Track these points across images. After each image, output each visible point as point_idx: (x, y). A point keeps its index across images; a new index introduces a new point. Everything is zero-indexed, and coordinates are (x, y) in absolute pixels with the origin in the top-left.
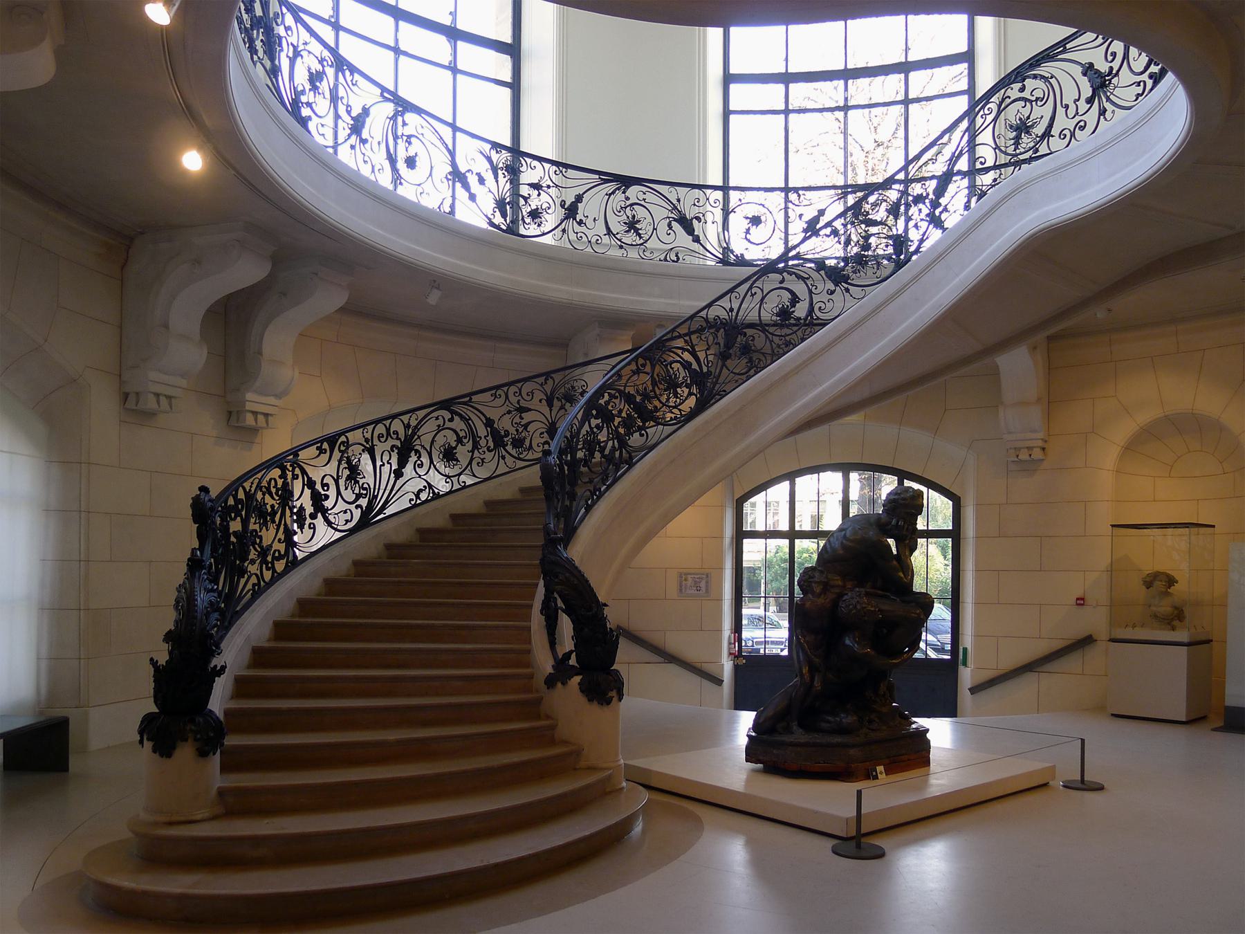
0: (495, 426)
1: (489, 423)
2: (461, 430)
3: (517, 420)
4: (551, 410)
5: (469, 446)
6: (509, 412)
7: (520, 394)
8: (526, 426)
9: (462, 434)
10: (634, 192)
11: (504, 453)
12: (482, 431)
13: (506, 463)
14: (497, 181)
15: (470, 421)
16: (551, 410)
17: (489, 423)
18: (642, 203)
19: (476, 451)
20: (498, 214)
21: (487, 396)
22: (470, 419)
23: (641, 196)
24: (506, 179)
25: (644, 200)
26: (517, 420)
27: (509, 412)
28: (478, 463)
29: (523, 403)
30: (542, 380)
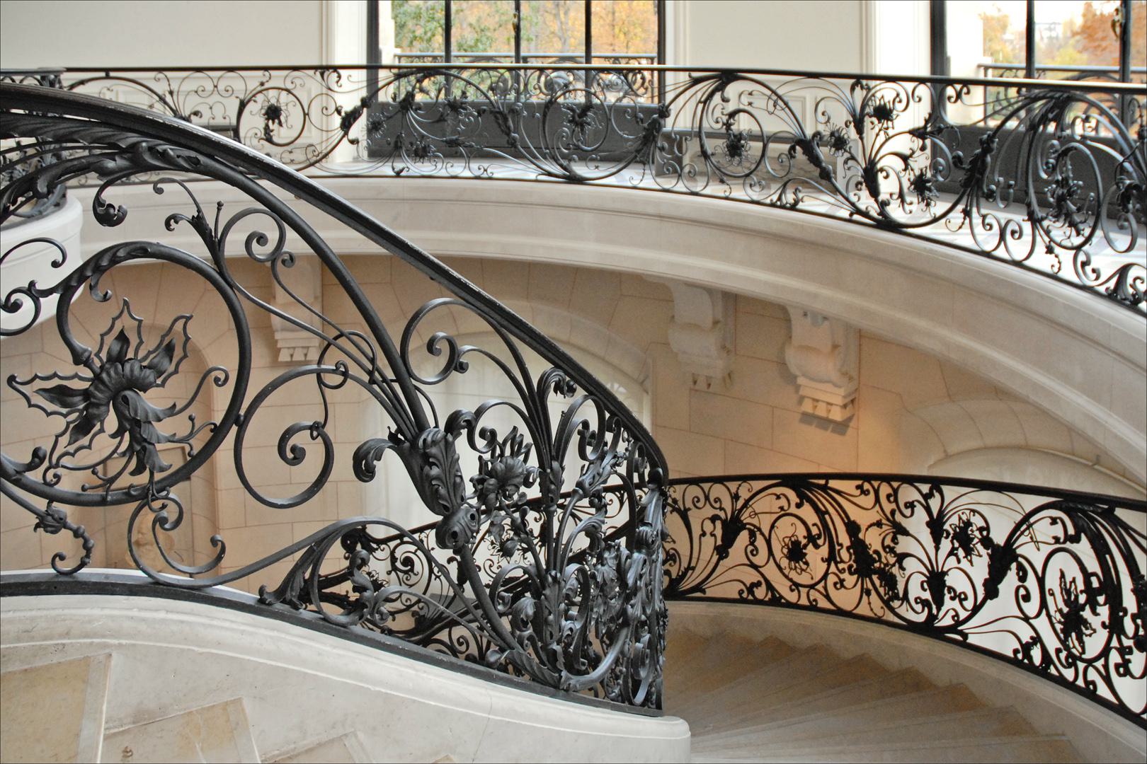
0: (861, 536)
1: (853, 528)
3: (888, 542)
4: (937, 548)
5: (824, 551)
7: (896, 501)
8: (901, 557)
9: (815, 531)
11: (870, 586)
12: (844, 539)
13: (869, 603)
14: (861, 138)
15: (827, 516)
16: (937, 548)
17: (853, 528)
19: (833, 564)
20: (865, 193)
21: (848, 486)
22: (827, 512)
24: (877, 130)
27: (879, 524)
28: (835, 584)
29: (898, 517)
30: (925, 488)
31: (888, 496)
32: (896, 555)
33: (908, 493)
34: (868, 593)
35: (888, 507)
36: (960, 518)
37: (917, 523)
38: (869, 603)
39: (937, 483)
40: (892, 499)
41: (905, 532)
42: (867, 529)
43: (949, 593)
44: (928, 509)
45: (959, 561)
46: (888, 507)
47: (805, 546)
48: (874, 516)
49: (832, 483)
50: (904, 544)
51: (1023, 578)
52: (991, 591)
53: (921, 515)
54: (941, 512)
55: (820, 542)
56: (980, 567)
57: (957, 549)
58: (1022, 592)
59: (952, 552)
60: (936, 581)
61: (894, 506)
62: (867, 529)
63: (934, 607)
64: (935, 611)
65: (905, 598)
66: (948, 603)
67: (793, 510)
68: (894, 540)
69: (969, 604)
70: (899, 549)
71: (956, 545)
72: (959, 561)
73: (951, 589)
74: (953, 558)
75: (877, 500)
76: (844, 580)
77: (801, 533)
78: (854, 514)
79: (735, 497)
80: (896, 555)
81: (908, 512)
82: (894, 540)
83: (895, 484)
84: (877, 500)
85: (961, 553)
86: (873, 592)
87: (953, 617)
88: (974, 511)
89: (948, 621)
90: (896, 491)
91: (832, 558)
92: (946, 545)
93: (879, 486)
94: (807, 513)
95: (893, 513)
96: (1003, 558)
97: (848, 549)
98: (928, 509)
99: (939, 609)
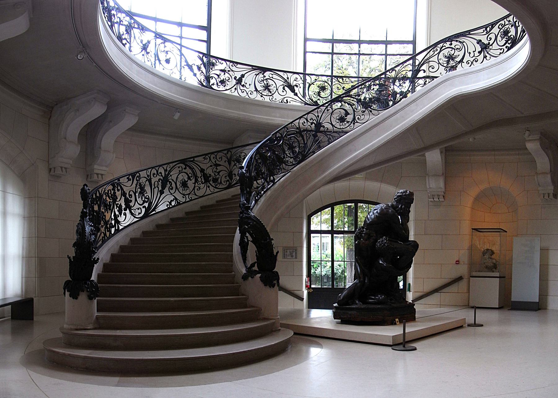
0: (205, 172)
1: (202, 170)
2: (190, 173)
3: (215, 170)
4: (230, 166)
5: (193, 181)
6: (211, 166)
7: (216, 158)
9: (190, 175)
10: (267, 74)
11: (209, 185)
13: (210, 190)
17: (202, 170)
18: (271, 78)
21: (201, 159)
22: (194, 168)
23: (271, 76)
25: (272, 77)
26: (215, 170)
29: (217, 162)
30: (225, 152)
31: (214, 157)
38: (210, 190)
42: (207, 169)
43: (234, 175)
46: (213, 161)
49: (196, 159)
54: (231, 157)
55: (192, 178)
57: (236, 163)
63: (230, 180)
64: (230, 182)
65: (221, 182)
67: (184, 170)
68: (217, 169)
70: (218, 171)
71: (236, 162)
75: (210, 159)
78: (203, 166)
79: (166, 171)
82: (217, 169)
86: (210, 186)
91: (196, 181)
93: (210, 156)
94: (188, 170)
97: (200, 177)
99: (231, 181)
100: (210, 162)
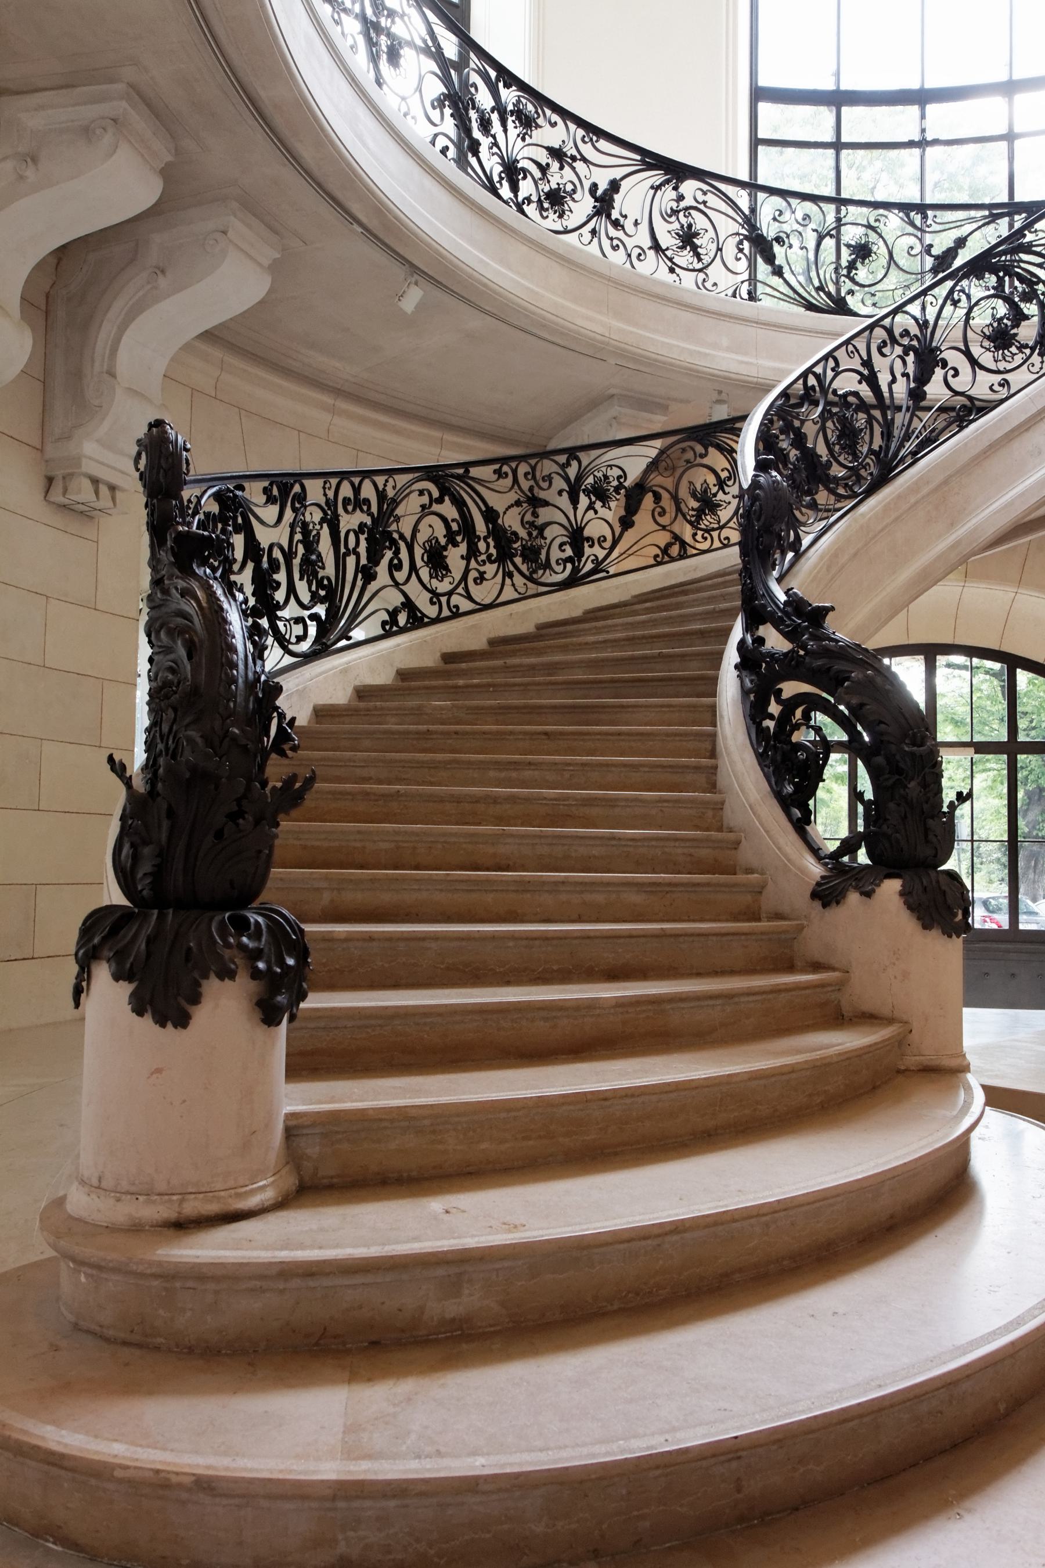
0: (500, 521)
3: (528, 517)
4: (575, 509)
5: (463, 549)
6: (518, 503)
7: (534, 477)
8: (541, 529)
11: (512, 568)
13: (513, 585)
30: (562, 459)
32: (536, 528)
33: (548, 467)
34: (511, 575)
35: (525, 484)
36: (595, 476)
37: (555, 493)
38: (513, 585)
39: (572, 453)
40: (530, 477)
41: (546, 503)
44: (567, 479)
45: (596, 512)
46: (525, 484)
47: (445, 548)
48: (513, 496)
50: (545, 514)
51: (657, 498)
52: (626, 523)
53: (559, 483)
54: (580, 477)
56: (613, 511)
57: (594, 503)
58: (658, 510)
59: (591, 507)
60: (577, 538)
61: (532, 483)
62: (505, 513)
66: (588, 551)
68: (535, 515)
69: (607, 544)
71: (593, 499)
72: (596, 512)
73: (588, 539)
74: (591, 512)
75: (515, 481)
76: (485, 572)
77: (440, 532)
80: (536, 528)
81: (545, 485)
83: (533, 462)
84: (515, 481)
85: (598, 505)
86: (515, 573)
87: (592, 561)
88: (611, 466)
89: (589, 566)
90: (534, 468)
91: (472, 552)
92: (584, 501)
95: (531, 489)
96: (635, 496)
98: (567, 479)
99: (579, 563)
100: (516, 487)
